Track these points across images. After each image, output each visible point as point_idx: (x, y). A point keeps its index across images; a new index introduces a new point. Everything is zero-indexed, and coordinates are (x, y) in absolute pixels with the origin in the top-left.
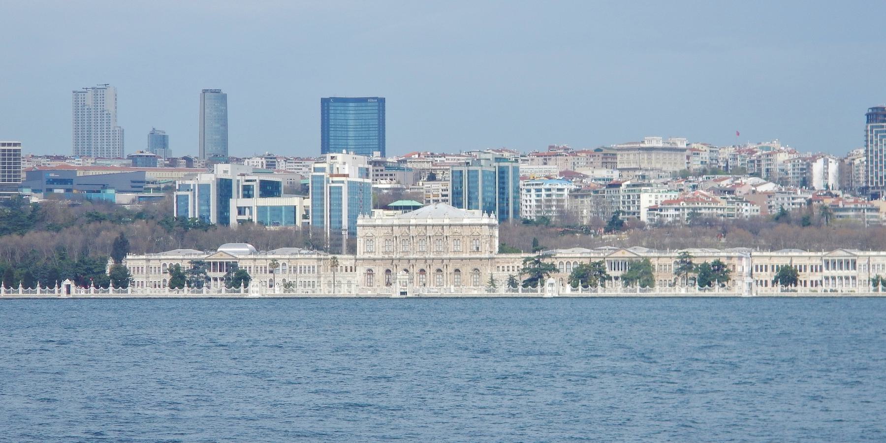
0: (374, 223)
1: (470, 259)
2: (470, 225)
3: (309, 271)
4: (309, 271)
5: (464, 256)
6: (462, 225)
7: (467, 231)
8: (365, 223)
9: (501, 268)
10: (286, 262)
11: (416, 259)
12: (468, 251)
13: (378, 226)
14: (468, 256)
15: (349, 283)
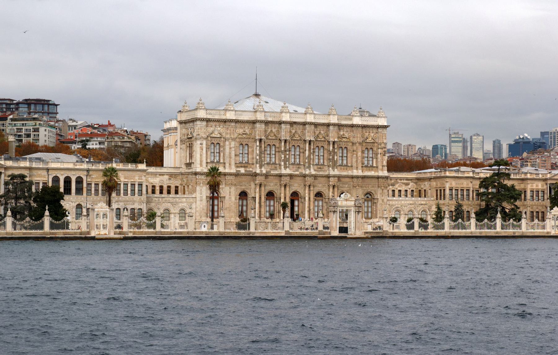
0: (224, 117)
1: (364, 177)
2: (364, 127)
3: (133, 191)
4: (133, 191)
5: (355, 173)
6: (352, 126)
7: (357, 137)
8: (209, 117)
9: (397, 192)
10: (83, 175)
11: (291, 176)
12: (360, 165)
13: (231, 121)
14: (359, 173)
15: (183, 213)
